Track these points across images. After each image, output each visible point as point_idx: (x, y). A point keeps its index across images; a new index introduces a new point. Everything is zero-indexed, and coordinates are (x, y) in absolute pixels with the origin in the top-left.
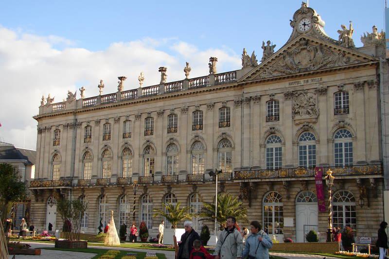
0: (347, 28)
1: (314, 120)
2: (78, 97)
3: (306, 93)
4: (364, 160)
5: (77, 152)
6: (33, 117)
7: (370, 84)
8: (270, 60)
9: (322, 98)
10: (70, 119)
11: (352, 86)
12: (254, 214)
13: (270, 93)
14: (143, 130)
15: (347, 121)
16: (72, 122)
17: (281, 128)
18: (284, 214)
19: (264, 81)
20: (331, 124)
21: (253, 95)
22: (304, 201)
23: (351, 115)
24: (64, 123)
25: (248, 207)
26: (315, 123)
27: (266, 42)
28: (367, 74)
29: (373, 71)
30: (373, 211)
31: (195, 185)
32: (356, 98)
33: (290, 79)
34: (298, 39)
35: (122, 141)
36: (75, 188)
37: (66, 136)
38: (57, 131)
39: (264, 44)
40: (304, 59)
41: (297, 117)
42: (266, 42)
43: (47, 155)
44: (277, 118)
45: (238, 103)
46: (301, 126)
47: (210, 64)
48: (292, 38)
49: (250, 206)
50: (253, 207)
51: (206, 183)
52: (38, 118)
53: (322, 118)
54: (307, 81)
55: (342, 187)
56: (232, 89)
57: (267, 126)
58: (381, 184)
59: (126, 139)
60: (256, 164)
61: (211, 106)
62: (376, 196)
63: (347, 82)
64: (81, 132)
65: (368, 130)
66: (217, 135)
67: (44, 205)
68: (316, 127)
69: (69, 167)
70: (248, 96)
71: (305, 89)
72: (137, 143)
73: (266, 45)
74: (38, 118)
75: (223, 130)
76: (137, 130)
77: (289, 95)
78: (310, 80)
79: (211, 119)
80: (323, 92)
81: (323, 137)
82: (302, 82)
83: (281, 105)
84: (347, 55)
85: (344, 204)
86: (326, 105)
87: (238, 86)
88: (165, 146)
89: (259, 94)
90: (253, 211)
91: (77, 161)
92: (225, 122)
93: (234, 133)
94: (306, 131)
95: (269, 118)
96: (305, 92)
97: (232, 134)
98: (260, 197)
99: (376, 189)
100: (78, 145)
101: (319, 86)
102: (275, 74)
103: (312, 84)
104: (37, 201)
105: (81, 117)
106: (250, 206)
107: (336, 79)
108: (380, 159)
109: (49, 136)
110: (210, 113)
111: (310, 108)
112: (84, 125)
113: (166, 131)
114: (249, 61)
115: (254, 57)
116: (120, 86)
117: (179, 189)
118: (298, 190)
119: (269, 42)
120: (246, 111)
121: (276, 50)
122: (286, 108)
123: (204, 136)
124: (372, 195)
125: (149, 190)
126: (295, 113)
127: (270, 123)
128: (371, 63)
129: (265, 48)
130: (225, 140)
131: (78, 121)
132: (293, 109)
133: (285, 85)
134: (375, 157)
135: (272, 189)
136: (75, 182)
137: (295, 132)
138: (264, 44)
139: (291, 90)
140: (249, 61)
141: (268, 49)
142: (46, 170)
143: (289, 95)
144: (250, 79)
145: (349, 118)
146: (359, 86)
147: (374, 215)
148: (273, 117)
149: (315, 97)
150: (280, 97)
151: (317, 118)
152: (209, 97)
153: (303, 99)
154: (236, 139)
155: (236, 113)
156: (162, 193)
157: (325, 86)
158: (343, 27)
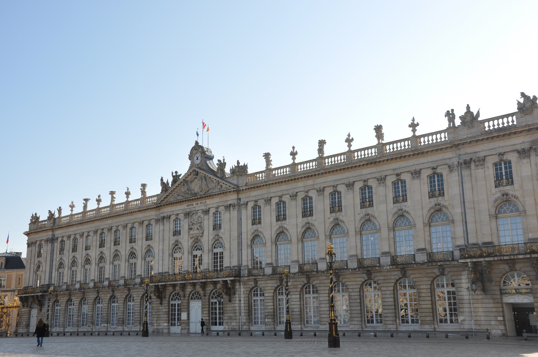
0: (222, 162)
1: (201, 235)
2: (57, 215)
3: (197, 213)
4: (229, 265)
6: (24, 233)
7: (234, 206)
8: (175, 187)
9: (206, 217)
10: (49, 234)
11: (223, 207)
12: (164, 310)
13: (175, 213)
14: (98, 243)
15: (220, 235)
16: (51, 237)
17: (182, 242)
18: (182, 310)
19: (171, 204)
21: (165, 215)
22: (195, 299)
23: (222, 231)
24: (45, 238)
25: (160, 305)
26: (201, 237)
27: (174, 172)
28: (232, 198)
29: (235, 196)
30: (233, 305)
31: (129, 288)
32: (225, 216)
33: (187, 202)
34: (191, 171)
37: (46, 249)
38: (40, 246)
39: (173, 173)
40: (196, 187)
41: (191, 232)
42: (174, 172)
43: (32, 266)
45: (157, 221)
46: (193, 239)
47: (141, 189)
48: (190, 168)
49: (161, 304)
50: (163, 305)
51: (136, 286)
52: (27, 234)
53: (206, 233)
54: (197, 204)
56: (154, 209)
57: (173, 239)
58: (238, 284)
60: (166, 270)
62: (235, 294)
63: (221, 205)
64: (57, 245)
65: (232, 242)
67: (27, 309)
68: (202, 240)
70: (162, 215)
71: (197, 209)
72: (94, 254)
73: (174, 174)
74: (27, 234)
76: (94, 243)
77: (187, 215)
78: (199, 202)
81: (206, 248)
82: (194, 203)
84: (221, 184)
86: (208, 222)
87: (157, 207)
88: (112, 256)
89: (169, 214)
90: (163, 308)
91: (54, 270)
94: (196, 245)
96: (197, 212)
98: (167, 296)
99: (234, 288)
101: (204, 208)
102: (179, 198)
104: (23, 306)
105: (58, 233)
106: (161, 304)
107: (214, 202)
108: (239, 264)
109: (35, 249)
111: (199, 225)
112: (60, 239)
113: (113, 244)
115: (168, 183)
116: (85, 207)
117: (119, 292)
118: (190, 290)
119: (176, 172)
122: (185, 224)
124: (232, 293)
125: (100, 293)
128: (233, 190)
129: (173, 176)
132: (189, 225)
133: (184, 207)
134: (235, 263)
136: (52, 288)
137: (190, 244)
138: (173, 173)
141: (176, 177)
144: (163, 202)
145: (221, 232)
146: (228, 207)
147: (233, 309)
149: (202, 216)
151: (203, 233)
153: (195, 217)
156: (109, 296)
157: (208, 208)
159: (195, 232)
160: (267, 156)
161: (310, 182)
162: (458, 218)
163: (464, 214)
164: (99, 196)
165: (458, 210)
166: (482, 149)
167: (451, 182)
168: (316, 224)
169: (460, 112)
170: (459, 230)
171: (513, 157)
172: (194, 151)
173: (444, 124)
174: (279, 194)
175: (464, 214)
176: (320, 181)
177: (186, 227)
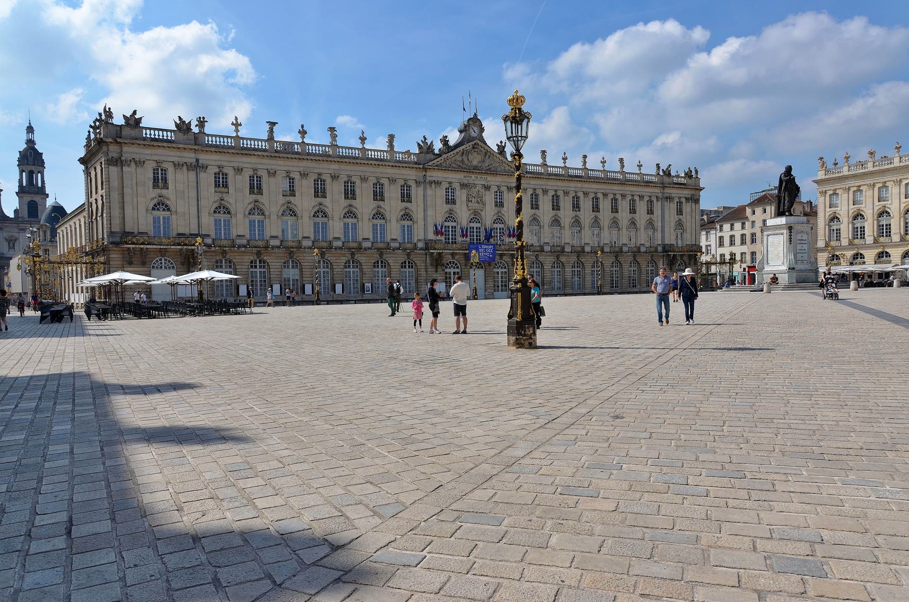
5: (203, 203)
17: (458, 211)
20: (493, 213)
23: (505, 208)
35: (282, 200)
36: (213, 249)
41: (470, 204)
44: (454, 202)
55: (501, 259)
59: (288, 198)
61: (392, 181)
64: (207, 178)
66: (399, 209)
68: (483, 213)
69: (194, 222)
70: (434, 179)
75: (405, 204)
79: (392, 193)
80: (487, 188)
83: (458, 192)
85: (500, 270)
86: (489, 198)
89: (440, 179)
92: (406, 197)
93: (416, 207)
95: (447, 202)
96: (475, 185)
97: (414, 209)
100: (204, 194)
102: (454, 165)
103: (478, 180)
105: (204, 158)
110: (393, 187)
114: (426, 148)
120: (429, 192)
121: (452, 143)
122: (461, 196)
123: (386, 207)
126: (468, 201)
127: (449, 206)
130: (407, 216)
131: (200, 162)
135: (453, 258)
139: (466, 182)
140: (426, 148)
142: (142, 221)
143: (463, 186)
148: (451, 201)
150: (456, 186)
152: (391, 171)
153: (474, 191)
154: (418, 215)
155: (417, 193)
156: (344, 260)
158: (501, 142)
159: (474, 205)
160: (544, 152)
161: (579, 185)
162: (660, 229)
163: (663, 227)
164: (302, 126)
165: (660, 224)
166: (674, 192)
167: (657, 207)
168: (582, 217)
169: (664, 167)
170: (659, 235)
171: (683, 200)
172: (471, 122)
173: (654, 172)
174: (555, 188)
175: (663, 227)
176: (587, 186)
177: (464, 198)
